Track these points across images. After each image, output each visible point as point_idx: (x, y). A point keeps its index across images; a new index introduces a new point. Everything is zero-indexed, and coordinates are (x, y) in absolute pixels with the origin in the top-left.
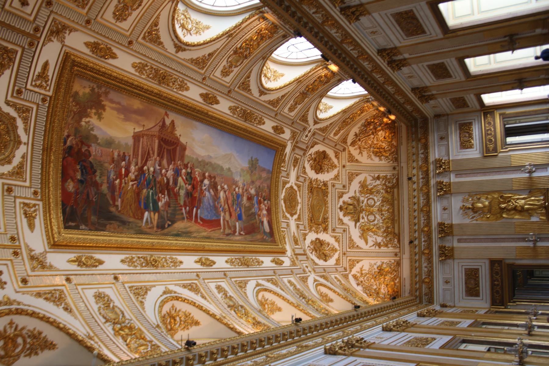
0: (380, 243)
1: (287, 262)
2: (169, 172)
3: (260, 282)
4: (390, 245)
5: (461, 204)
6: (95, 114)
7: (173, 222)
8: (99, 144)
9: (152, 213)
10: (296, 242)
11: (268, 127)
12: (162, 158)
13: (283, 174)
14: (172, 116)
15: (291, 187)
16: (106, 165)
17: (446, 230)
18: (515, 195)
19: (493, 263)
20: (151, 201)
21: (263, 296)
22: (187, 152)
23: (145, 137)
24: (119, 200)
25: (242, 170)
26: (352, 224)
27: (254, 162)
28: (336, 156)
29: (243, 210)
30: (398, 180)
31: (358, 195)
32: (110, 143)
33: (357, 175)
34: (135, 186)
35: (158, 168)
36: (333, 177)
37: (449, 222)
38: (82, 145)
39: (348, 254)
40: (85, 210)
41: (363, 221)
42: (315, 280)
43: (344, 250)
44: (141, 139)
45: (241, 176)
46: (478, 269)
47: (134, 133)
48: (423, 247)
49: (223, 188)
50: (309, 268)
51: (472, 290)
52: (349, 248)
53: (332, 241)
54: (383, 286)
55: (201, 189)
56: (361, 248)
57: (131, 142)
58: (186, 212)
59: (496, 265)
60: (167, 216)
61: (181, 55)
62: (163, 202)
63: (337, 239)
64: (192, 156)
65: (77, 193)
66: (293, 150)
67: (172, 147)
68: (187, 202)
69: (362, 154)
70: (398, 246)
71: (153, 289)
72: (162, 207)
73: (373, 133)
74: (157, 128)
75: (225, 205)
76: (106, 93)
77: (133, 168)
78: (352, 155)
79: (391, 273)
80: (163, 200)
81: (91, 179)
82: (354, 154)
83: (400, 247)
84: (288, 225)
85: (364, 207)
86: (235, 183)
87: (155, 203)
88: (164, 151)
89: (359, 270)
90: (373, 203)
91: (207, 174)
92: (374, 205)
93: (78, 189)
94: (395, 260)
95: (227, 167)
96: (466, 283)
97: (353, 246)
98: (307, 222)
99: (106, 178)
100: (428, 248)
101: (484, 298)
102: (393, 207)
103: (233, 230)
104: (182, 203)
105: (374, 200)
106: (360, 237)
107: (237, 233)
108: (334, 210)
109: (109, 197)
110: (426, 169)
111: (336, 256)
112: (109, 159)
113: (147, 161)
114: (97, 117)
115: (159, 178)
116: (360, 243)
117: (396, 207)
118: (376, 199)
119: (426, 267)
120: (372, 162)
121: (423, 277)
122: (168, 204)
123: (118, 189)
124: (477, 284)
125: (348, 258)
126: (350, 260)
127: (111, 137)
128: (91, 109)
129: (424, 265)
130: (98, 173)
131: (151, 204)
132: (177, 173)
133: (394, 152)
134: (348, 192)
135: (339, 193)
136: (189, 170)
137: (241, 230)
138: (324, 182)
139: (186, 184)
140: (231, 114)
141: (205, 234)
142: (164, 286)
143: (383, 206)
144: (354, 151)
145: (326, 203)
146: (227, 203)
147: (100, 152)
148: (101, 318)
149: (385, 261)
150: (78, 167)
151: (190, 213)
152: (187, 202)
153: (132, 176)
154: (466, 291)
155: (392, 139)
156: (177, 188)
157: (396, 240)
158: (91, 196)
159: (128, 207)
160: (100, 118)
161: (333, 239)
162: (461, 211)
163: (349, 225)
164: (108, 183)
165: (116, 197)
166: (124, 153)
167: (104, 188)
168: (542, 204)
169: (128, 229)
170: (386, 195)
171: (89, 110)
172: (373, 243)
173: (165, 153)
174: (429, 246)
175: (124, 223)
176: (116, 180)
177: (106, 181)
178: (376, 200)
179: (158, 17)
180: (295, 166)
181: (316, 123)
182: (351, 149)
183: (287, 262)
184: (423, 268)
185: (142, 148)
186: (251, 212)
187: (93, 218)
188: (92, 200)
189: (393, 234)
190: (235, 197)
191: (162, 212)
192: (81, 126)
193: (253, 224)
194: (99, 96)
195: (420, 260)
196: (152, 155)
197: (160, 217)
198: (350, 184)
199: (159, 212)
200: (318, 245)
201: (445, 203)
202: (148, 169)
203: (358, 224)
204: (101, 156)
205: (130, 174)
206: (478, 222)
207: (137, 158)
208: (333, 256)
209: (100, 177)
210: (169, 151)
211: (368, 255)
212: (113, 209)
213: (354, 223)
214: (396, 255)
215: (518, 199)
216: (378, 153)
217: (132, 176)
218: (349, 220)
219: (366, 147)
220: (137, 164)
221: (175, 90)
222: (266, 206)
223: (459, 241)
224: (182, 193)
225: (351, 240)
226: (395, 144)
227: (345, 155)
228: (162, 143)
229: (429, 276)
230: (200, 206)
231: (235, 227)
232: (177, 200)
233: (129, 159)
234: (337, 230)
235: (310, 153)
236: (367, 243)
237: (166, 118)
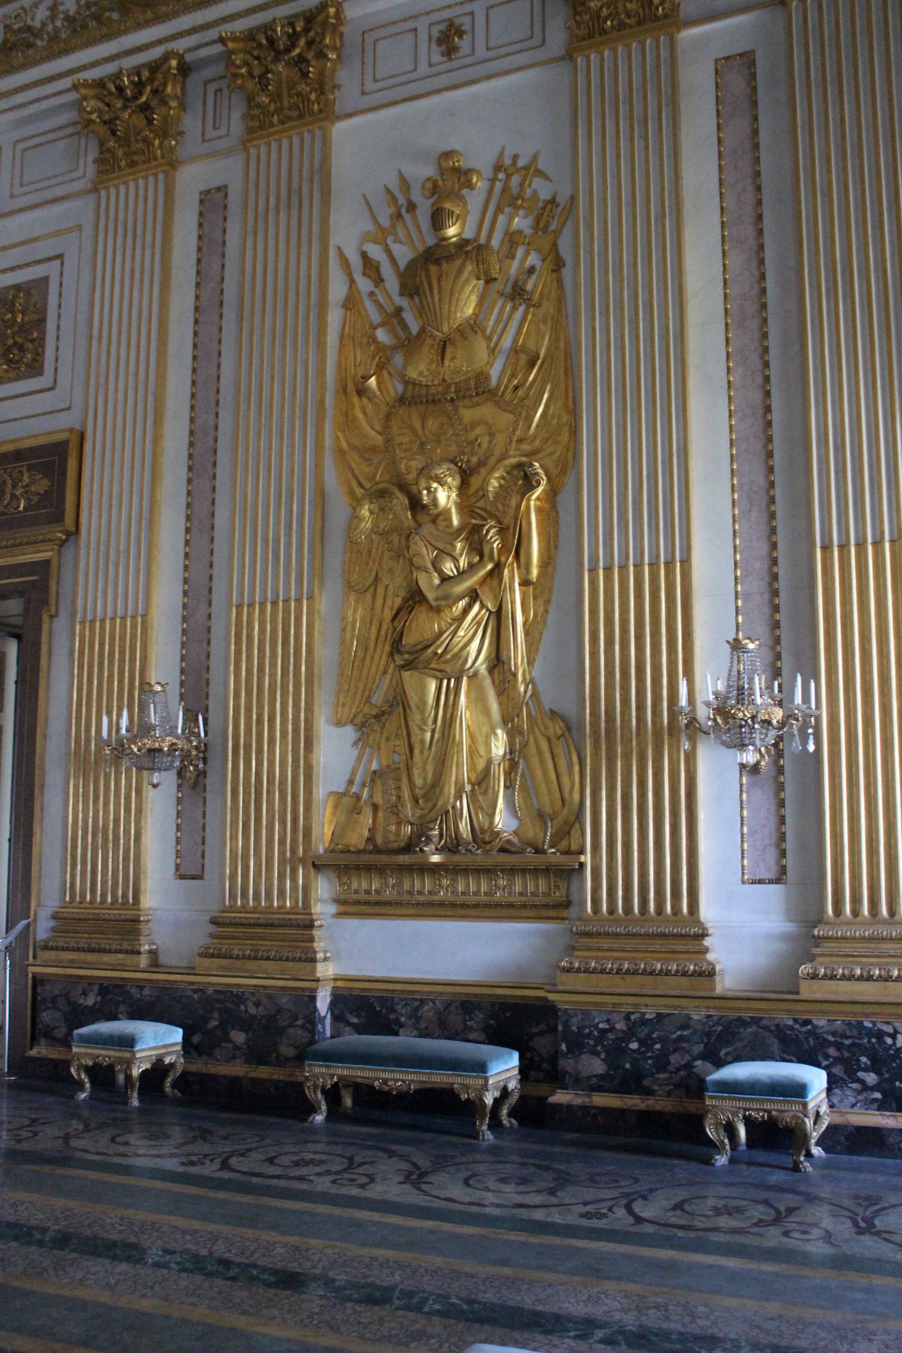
5: (479, 151)
18: (538, 591)
37: (347, 94)
46: (36, 368)
59: (42, 485)
162: (429, 171)
168: (448, 816)
206: (334, 317)
215: (499, 618)
223: (213, 202)
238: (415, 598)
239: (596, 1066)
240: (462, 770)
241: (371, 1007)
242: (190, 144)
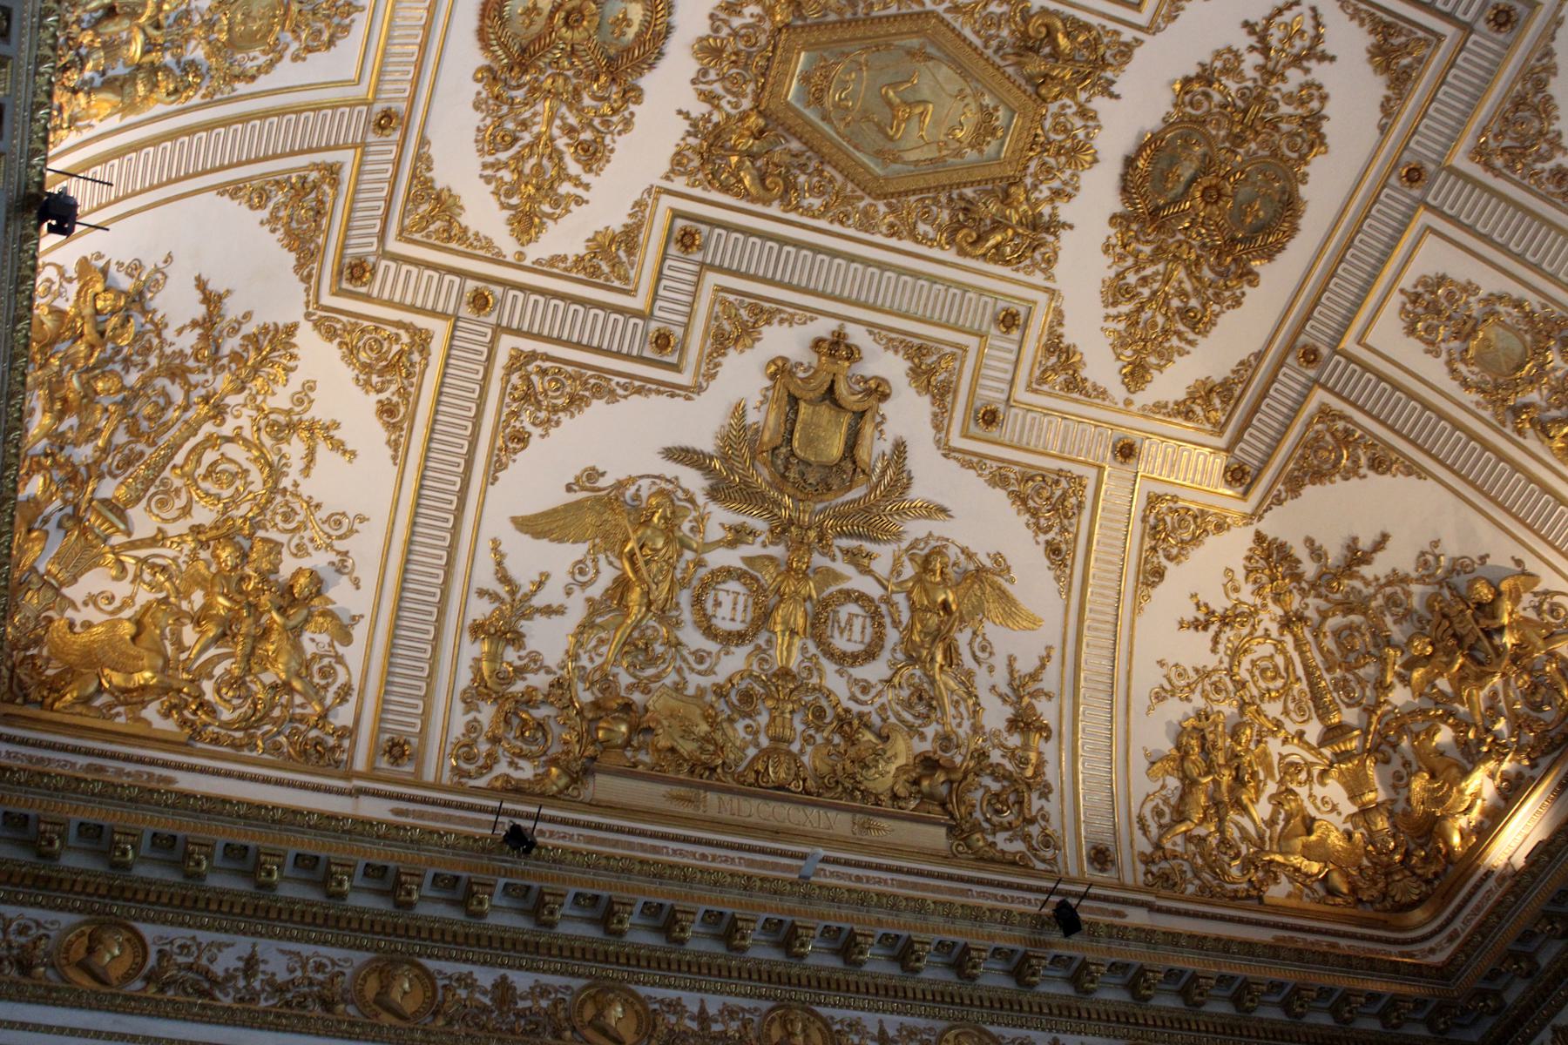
0: (517, 639)
4: (487, 713)
26: (701, 423)
31: (915, 529)
36: (1070, 335)
39: (476, 330)
41: (714, 532)
43: (515, 309)
48: (450, 968)
52: (520, 360)
53: (606, 199)
56: (496, 466)
63: (611, 253)
69: (1199, 625)
70: (482, 782)
73: (1333, 733)
79: (237, 683)
82: (1196, 555)
85: (818, 560)
89: (319, 411)
90: (841, 643)
92: (830, 654)
94: (349, 733)
97: (529, 396)
102: (808, 798)
105: (870, 654)
106: (593, 474)
116: (541, 474)
118: (875, 671)
121: (148, 931)
126: (422, 340)
129: (276, 959)
133: (1219, 872)
134: (949, 452)
138: (1055, 226)
149: (353, 654)
157: (527, 771)
161: (617, 220)
163: (699, 400)
170: (904, 751)
172: (524, 576)
178: (859, 672)
184: (243, 945)
195: (330, 922)
203: (693, 480)
211: (438, 510)
213: (706, 443)
218: (739, 411)
219: (1246, 661)
226: (1278, 891)
234: (681, 268)
236: (535, 526)
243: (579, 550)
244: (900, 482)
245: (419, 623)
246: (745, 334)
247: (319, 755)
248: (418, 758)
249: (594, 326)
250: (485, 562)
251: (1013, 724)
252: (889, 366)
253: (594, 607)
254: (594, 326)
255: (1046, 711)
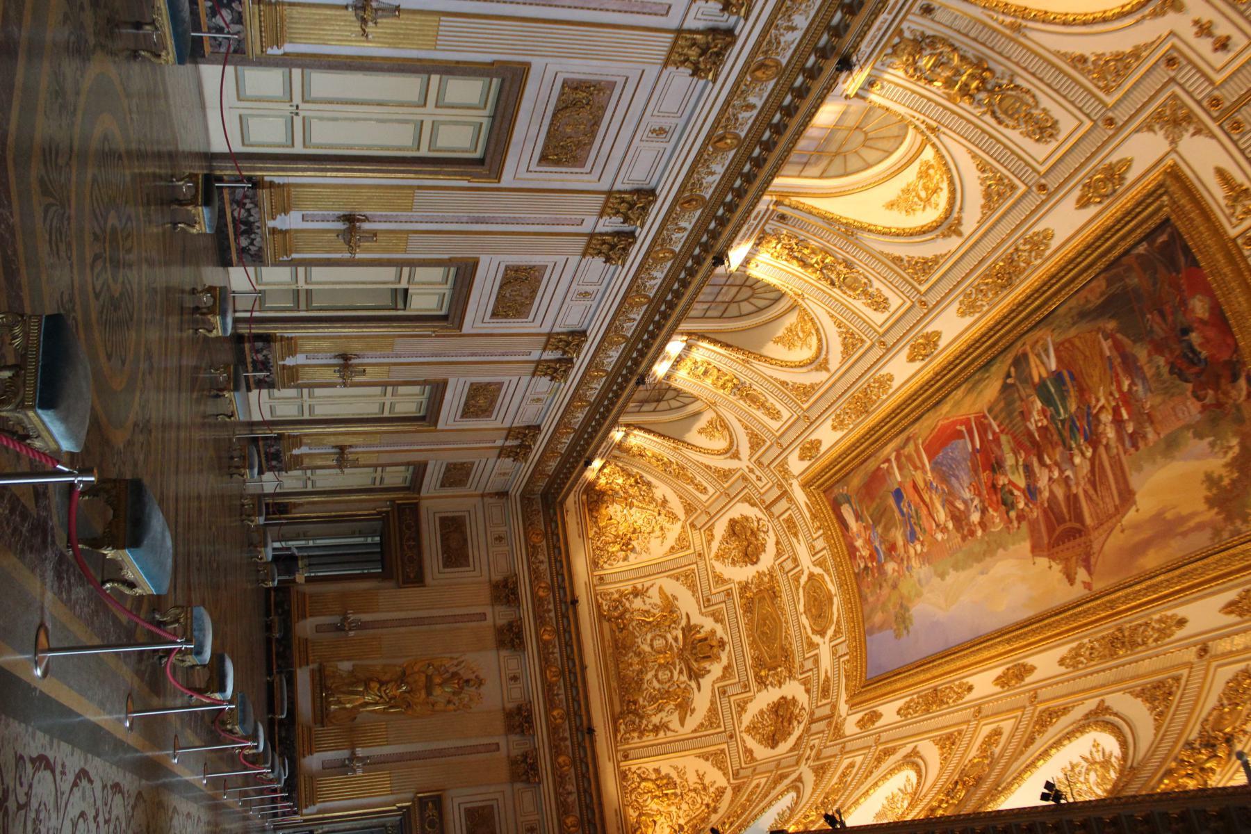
0: (636, 596)
1: (796, 465)
2: (1046, 479)
3: (823, 376)
4: (616, 596)
6: (1221, 478)
7: (1005, 388)
8: (1188, 427)
9: (1044, 375)
10: (791, 525)
11: (889, 711)
12: (1067, 498)
13: (843, 649)
14: (1078, 591)
15: (822, 633)
16: (1158, 400)
17: (510, 637)
19: (417, 579)
20: (1056, 397)
21: (810, 348)
22: (1026, 545)
23: (1112, 510)
24: (1108, 353)
25: (919, 595)
26: (696, 619)
27: (902, 627)
28: (751, 752)
29: (897, 514)
30: (616, 730)
31: (693, 684)
32: (1171, 446)
33: (702, 724)
34: (1094, 402)
35: (1069, 473)
36: (750, 706)
37: (503, 653)
38: (1217, 400)
40: (1155, 284)
42: (736, 456)
44: (1117, 502)
45: (919, 581)
46: (445, 566)
47: (1135, 503)
49: (944, 529)
50: (754, 477)
51: (453, 527)
54: (618, 517)
55: (979, 495)
57: (1134, 480)
58: (990, 425)
60: (1018, 390)
61: (1091, 704)
62: (1035, 413)
63: (720, 580)
64: (1017, 546)
65: (1183, 303)
66: (834, 707)
67: (1057, 532)
68: (995, 449)
71: (979, 216)
72: (1032, 403)
74: (1096, 547)
75: (931, 498)
76: (1217, 532)
77: (1111, 433)
78: (720, 768)
79: (607, 543)
80: (1037, 418)
81: (1172, 352)
83: (596, 595)
84: (812, 547)
86: (924, 558)
87: (1047, 400)
88: (1069, 512)
89: (668, 534)
90: (660, 674)
91: (979, 533)
93: (1185, 313)
95: (947, 578)
96: (466, 540)
97: (687, 576)
98: (782, 584)
99: (1148, 375)
100: (541, 598)
101: (431, 516)
103: (903, 459)
104: (1003, 438)
105: (658, 681)
107: (893, 458)
108: (736, 636)
109: (1126, 341)
110: (561, 759)
111: (715, 545)
112: (1158, 416)
113: (1092, 471)
114: (1215, 475)
115: (1058, 454)
117: (612, 672)
118: (657, 685)
119: (542, 562)
120: (675, 762)
122: (1025, 415)
123: (1119, 370)
124: (445, 539)
125: (692, 551)
126: (688, 547)
127: (1173, 458)
128: (1233, 482)
129: (544, 567)
130: (1165, 370)
131: (1053, 390)
132: (1031, 492)
135: (731, 676)
136: (1013, 514)
137: (889, 471)
138: (766, 687)
139: (1010, 482)
140: (964, 681)
141: (945, 408)
142: (966, 234)
143: (641, 672)
144: (716, 778)
145: (753, 644)
146: (927, 506)
147: (1180, 415)
148: (1025, 85)
149: (621, 563)
150: (1204, 354)
151: (983, 429)
152: (995, 449)
153: (1106, 417)
154: (465, 525)
155: (638, 822)
156: (1021, 462)
157: (605, 608)
158: (1158, 319)
159: (1088, 354)
160: (1210, 480)
161: (726, 577)
162: (482, 677)
164: (1141, 368)
165: (1115, 353)
166: (1137, 449)
167: (1141, 353)
168: (333, 695)
169: (1071, 309)
171: (1236, 475)
172: (650, 592)
173: (1065, 510)
174: (538, 603)
175: (1083, 315)
176: (1130, 386)
177: (1146, 368)
179: (1158, 728)
180: (827, 679)
181: (799, 779)
182: (722, 781)
183: (796, 465)
185: (1109, 488)
186: (882, 524)
187: (1134, 280)
188: (1151, 313)
189: (615, 618)
190: (917, 529)
191: (1029, 391)
192: (1235, 434)
193: (872, 499)
194: (1229, 518)
196: (1088, 487)
197: (1027, 379)
198: (713, 703)
199: (1034, 386)
200: (750, 555)
201: (516, 693)
202: (1083, 454)
203: (684, 623)
204: (1173, 409)
205: (1110, 418)
207: (1110, 458)
208: (721, 543)
209: (1158, 367)
210: (1061, 520)
211: (657, 570)
212: (1111, 325)
214: (601, 578)
215: (376, 704)
216: (665, 784)
217: (1106, 417)
219: (693, 794)
220: (1107, 447)
221: (1086, 640)
222: (862, 557)
223: (483, 616)
224: (1010, 460)
225: (692, 587)
226: (631, 811)
227: (733, 763)
228: (1077, 525)
229: (534, 547)
230: (971, 461)
231: (900, 468)
232: (1014, 438)
233: (1123, 445)
234: (722, 597)
235: (802, 726)
237: (1087, 579)
238: (382, 683)
239: (283, 734)
240: (343, 698)
241: (291, 682)
242: (498, 608)
243: (659, 602)
244: (703, 676)
245: (631, 575)
246: (716, 621)
247: (595, 564)
248: (601, 584)
249: (705, 584)
250: (649, 584)
251: (655, 726)
252: (724, 656)
253: (648, 612)
254: (705, 584)
255: (662, 734)
